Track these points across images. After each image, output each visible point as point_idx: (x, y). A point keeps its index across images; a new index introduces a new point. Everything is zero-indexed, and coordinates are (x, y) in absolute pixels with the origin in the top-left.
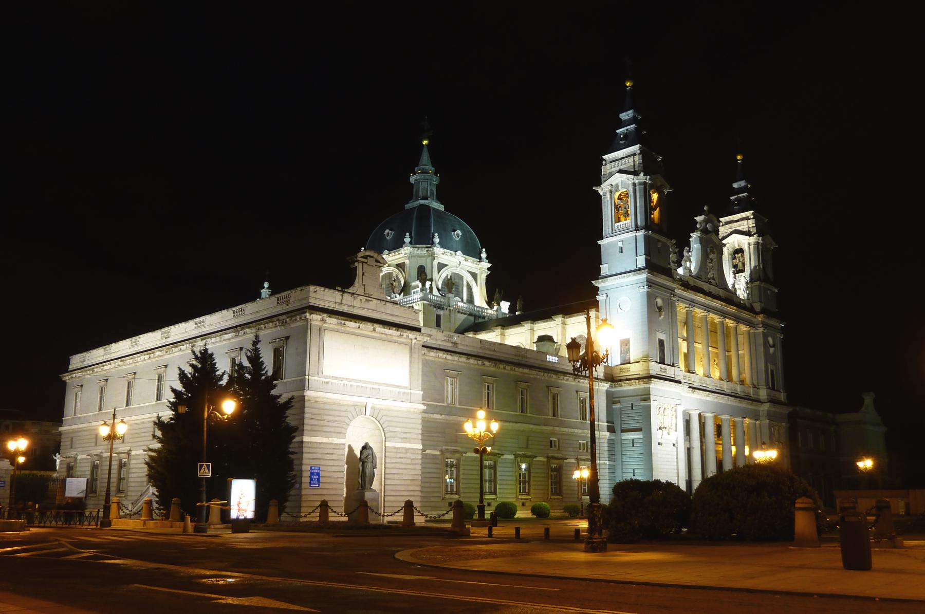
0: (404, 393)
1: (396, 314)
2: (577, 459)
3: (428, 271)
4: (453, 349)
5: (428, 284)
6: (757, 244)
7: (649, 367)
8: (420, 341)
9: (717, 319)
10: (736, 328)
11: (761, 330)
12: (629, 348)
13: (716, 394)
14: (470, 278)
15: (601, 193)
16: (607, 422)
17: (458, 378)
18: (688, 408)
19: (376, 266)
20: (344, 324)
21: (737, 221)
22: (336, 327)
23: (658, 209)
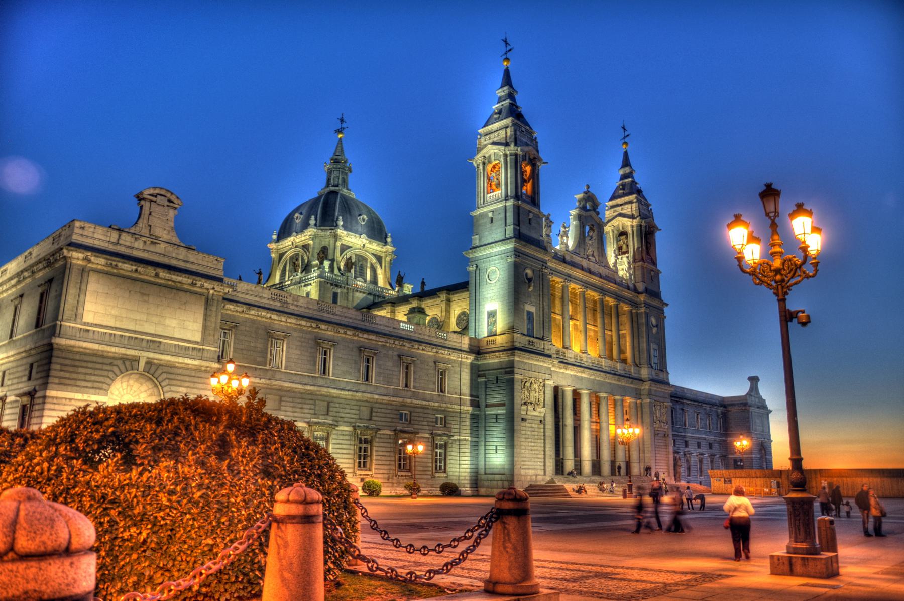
0: (194, 349)
1: (191, 260)
2: (432, 434)
3: (331, 251)
4: (281, 309)
5: (327, 264)
6: (641, 226)
7: (513, 338)
8: (219, 292)
9: (596, 296)
10: (617, 306)
11: (643, 310)
12: (495, 321)
13: (592, 371)
14: (374, 260)
15: (475, 165)
16: (471, 396)
17: (286, 340)
18: (577, 387)
19: (168, 206)
20: (116, 266)
21: (622, 205)
22: (106, 269)
23: (531, 181)
